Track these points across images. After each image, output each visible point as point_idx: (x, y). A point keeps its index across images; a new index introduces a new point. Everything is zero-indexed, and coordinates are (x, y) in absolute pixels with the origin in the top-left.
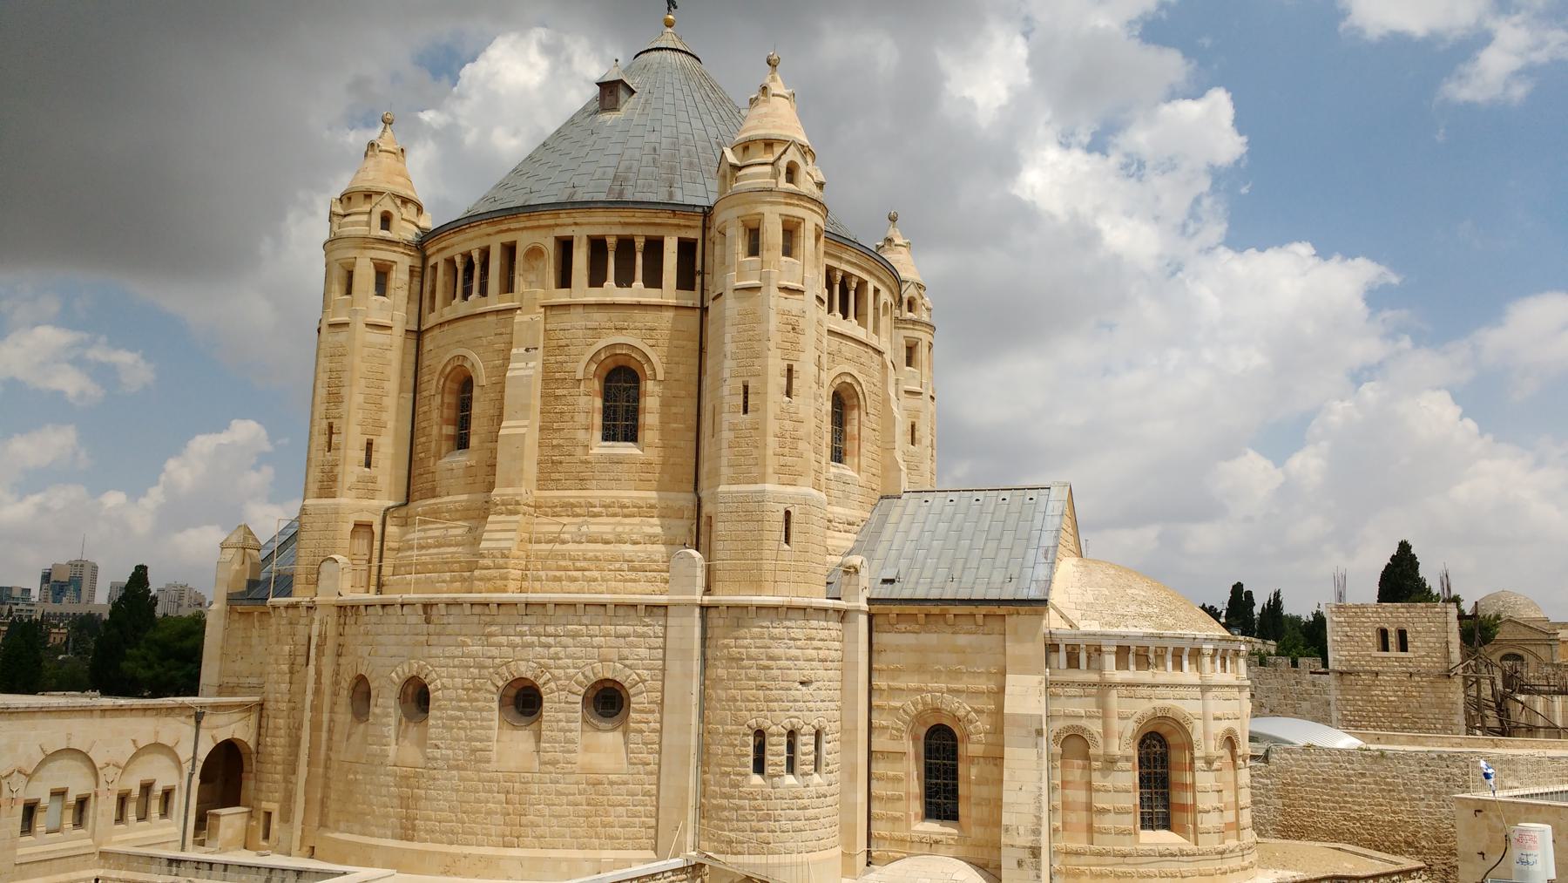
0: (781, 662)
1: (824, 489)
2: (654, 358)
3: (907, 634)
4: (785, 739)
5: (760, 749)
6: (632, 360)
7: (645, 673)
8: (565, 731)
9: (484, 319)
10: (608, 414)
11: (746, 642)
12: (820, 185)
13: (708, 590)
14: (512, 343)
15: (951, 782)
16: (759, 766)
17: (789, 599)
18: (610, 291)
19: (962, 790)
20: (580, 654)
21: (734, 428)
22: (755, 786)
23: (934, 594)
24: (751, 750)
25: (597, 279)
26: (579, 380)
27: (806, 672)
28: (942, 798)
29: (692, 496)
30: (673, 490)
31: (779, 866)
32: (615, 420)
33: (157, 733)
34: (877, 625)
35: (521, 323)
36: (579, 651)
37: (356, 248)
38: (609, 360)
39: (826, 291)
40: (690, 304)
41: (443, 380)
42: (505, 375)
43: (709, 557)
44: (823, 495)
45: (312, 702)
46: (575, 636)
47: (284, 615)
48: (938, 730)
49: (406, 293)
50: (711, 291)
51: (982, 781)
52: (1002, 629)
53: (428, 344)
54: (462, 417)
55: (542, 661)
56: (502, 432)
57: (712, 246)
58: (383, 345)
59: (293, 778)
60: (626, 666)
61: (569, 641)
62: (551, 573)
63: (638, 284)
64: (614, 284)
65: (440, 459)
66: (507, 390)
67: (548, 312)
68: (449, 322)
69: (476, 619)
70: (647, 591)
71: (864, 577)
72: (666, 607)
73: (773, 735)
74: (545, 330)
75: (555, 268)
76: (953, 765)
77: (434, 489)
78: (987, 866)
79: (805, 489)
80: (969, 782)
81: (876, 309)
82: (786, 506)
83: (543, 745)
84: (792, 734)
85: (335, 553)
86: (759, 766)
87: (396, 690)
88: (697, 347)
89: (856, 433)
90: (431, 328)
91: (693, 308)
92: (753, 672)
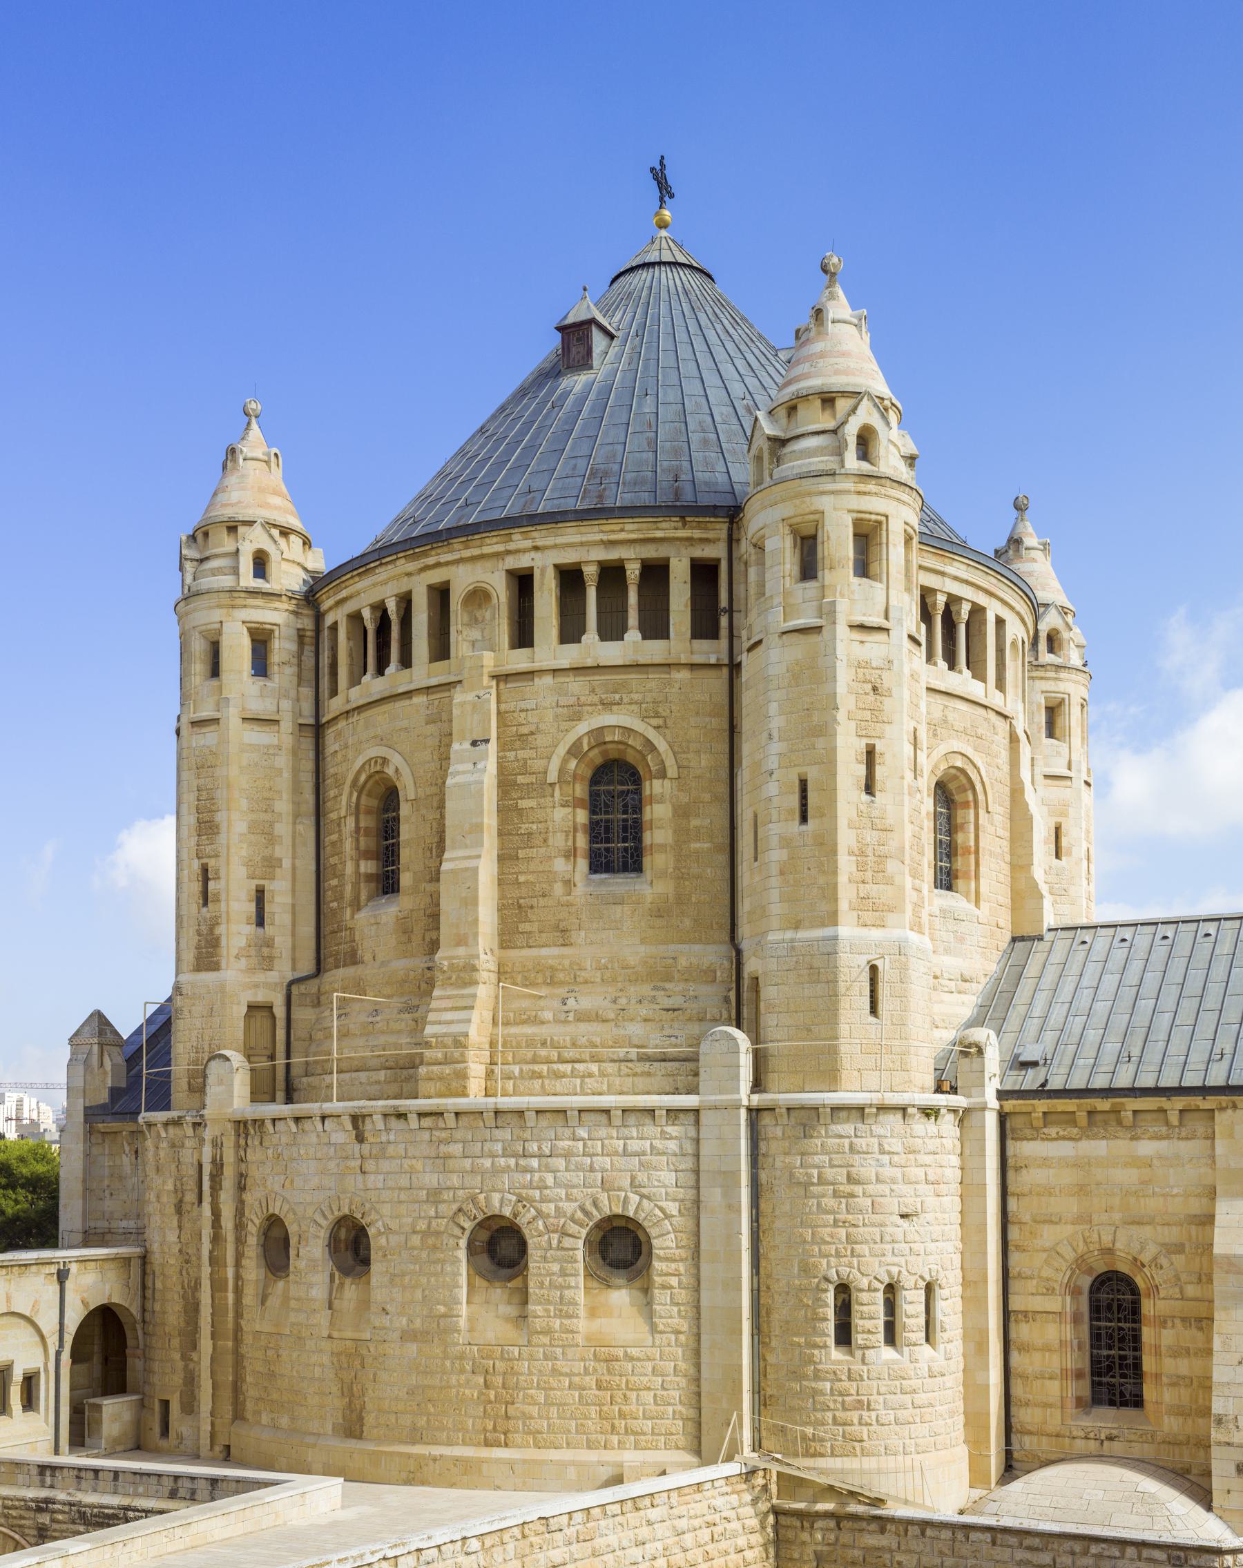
0: (870, 1187)
1: (927, 931)
2: (662, 745)
3: (1061, 1142)
4: (880, 1297)
5: (844, 1310)
6: (629, 750)
7: (673, 1208)
8: (561, 1287)
9: (407, 702)
10: (597, 831)
11: (817, 1159)
12: (911, 460)
13: (758, 1085)
14: (451, 734)
15: (1132, 1353)
16: (844, 1336)
17: (879, 1095)
18: (593, 649)
19: (1148, 1364)
20: (575, 1181)
21: (786, 842)
22: (839, 1362)
23: (1100, 1082)
24: (830, 1313)
25: (570, 632)
26: (551, 785)
27: (909, 1201)
28: (1117, 1375)
29: (725, 949)
30: (700, 941)
31: (879, 1472)
32: (608, 841)
33: (8, 1299)
34: (1013, 1130)
35: (462, 704)
36: (577, 1178)
37: (220, 607)
38: (596, 751)
39: (923, 627)
40: (713, 661)
41: (355, 794)
42: (444, 783)
43: (756, 1038)
44: (926, 939)
45: (211, 1252)
46: (567, 1155)
47: (163, 1135)
48: (1109, 1279)
49: (295, 669)
50: (744, 637)
51: (1179, 1352)
52: (1210, 1130)
53: (332, 744)
54: (387, 848)
55: (524, 1192)
56: (445, 866)
57: (743, 568)
58: (268, 747)
59: (194, 1356)
60: (642, 1196)
61: (560, 1163)
62: (526, 1067)
63: (633, 635)
64: (597, 637)
65: (359, 909)
66: (448, 804)
67: (502, 686)
68: (360, 709)
69: (426, 1135)
70: (668, 1089)
71: (993, 1060)
72: (697, 1111)
73: (861, 1290)
74: (499, 713)
75: (509, 618)
76: (1134, 1330)
77: (353, 953)
78: (1188, 1471)
79: (897, 931)
80: (1157, 1352)
81: (1000, 651)
82: (870, 957)
83: (531, 1307)
84: (891, 1289)
85: (225, 1048)
86: (844, 1336)
87: (324, 1234)
88: (723, 723)
89: (972, 843)
90: (335, 718)
91: (717, 666)
92: (829, 1202)
